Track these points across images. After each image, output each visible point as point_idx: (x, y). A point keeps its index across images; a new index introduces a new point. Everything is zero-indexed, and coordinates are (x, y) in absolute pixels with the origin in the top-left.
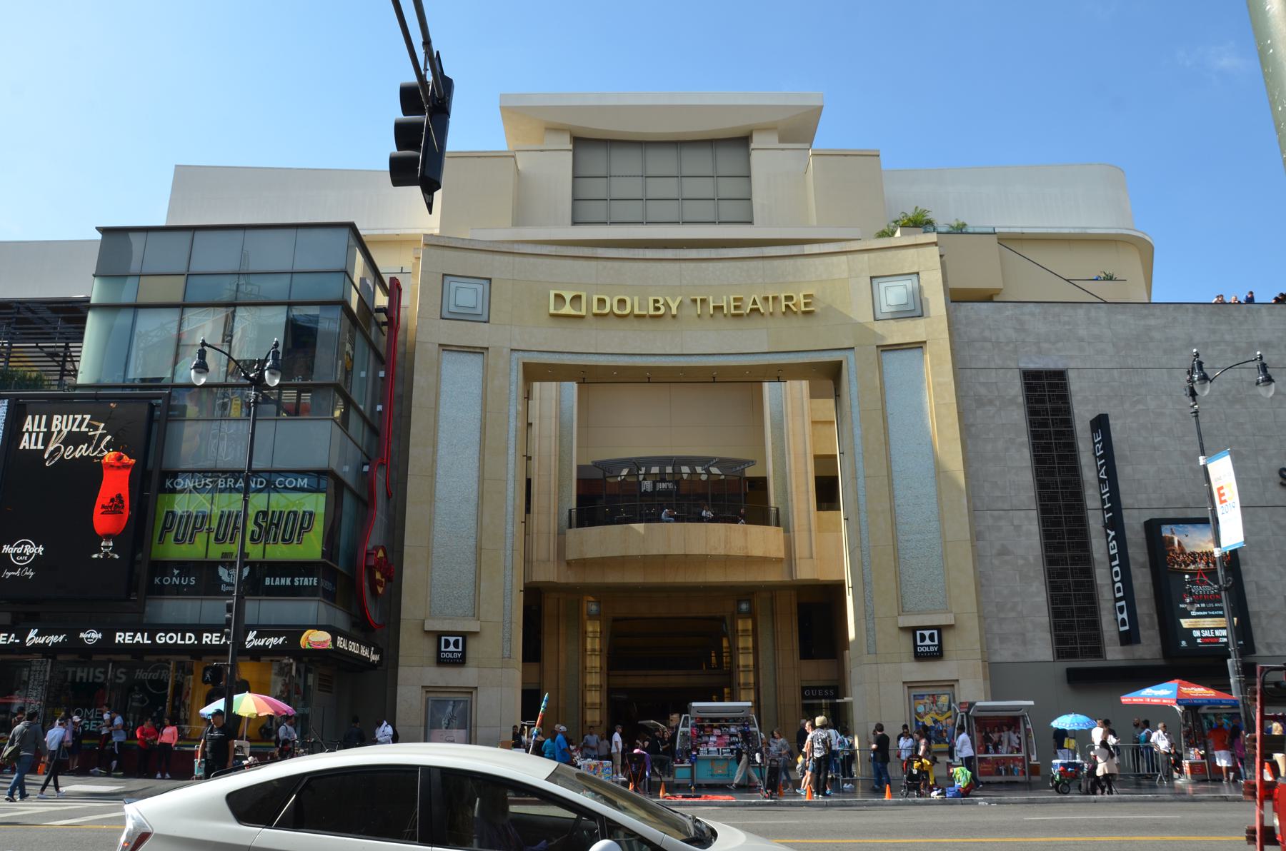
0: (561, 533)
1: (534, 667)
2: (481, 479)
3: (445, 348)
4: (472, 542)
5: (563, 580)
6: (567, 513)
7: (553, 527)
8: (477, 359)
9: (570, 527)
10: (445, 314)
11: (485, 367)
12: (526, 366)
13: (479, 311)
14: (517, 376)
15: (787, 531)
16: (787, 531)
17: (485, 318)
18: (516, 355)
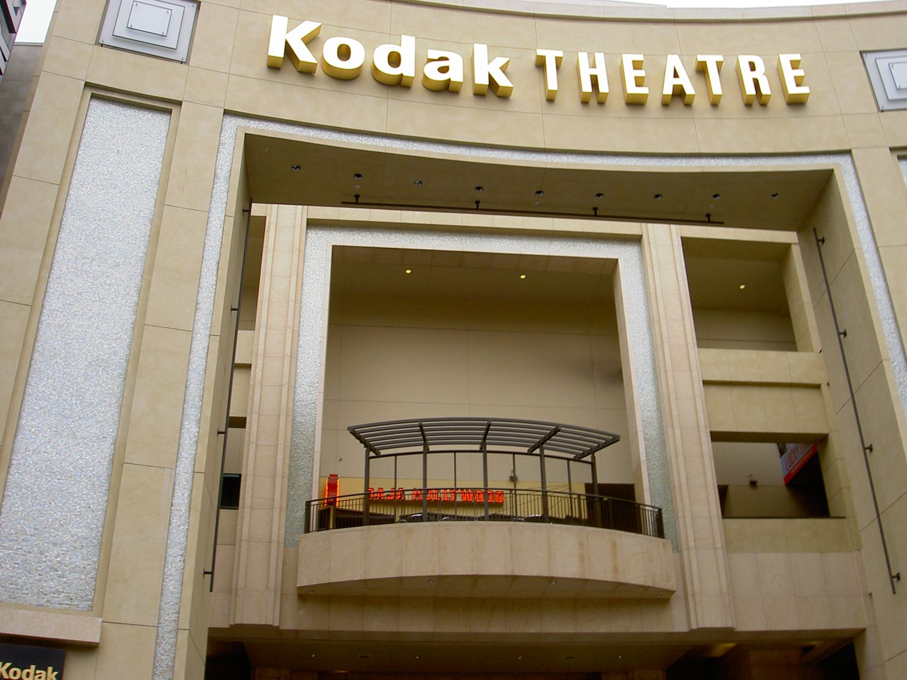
0: (290, 546)
1: (230, 470)
2: (140, 327)
3: (100, 93)
4: (107, 447)
5: (289, 625)
6: (301, 513)
7: (278, 532)
8: (159, 122)
9: (307, 530)
10: (106, 38)
11: (172, 135)
12: (254, 146)
13: (171, 42)
14: (229, 161)
15: (677, 549)
16: (677, 549)
17: (181, 55)
18: (232, 122)
